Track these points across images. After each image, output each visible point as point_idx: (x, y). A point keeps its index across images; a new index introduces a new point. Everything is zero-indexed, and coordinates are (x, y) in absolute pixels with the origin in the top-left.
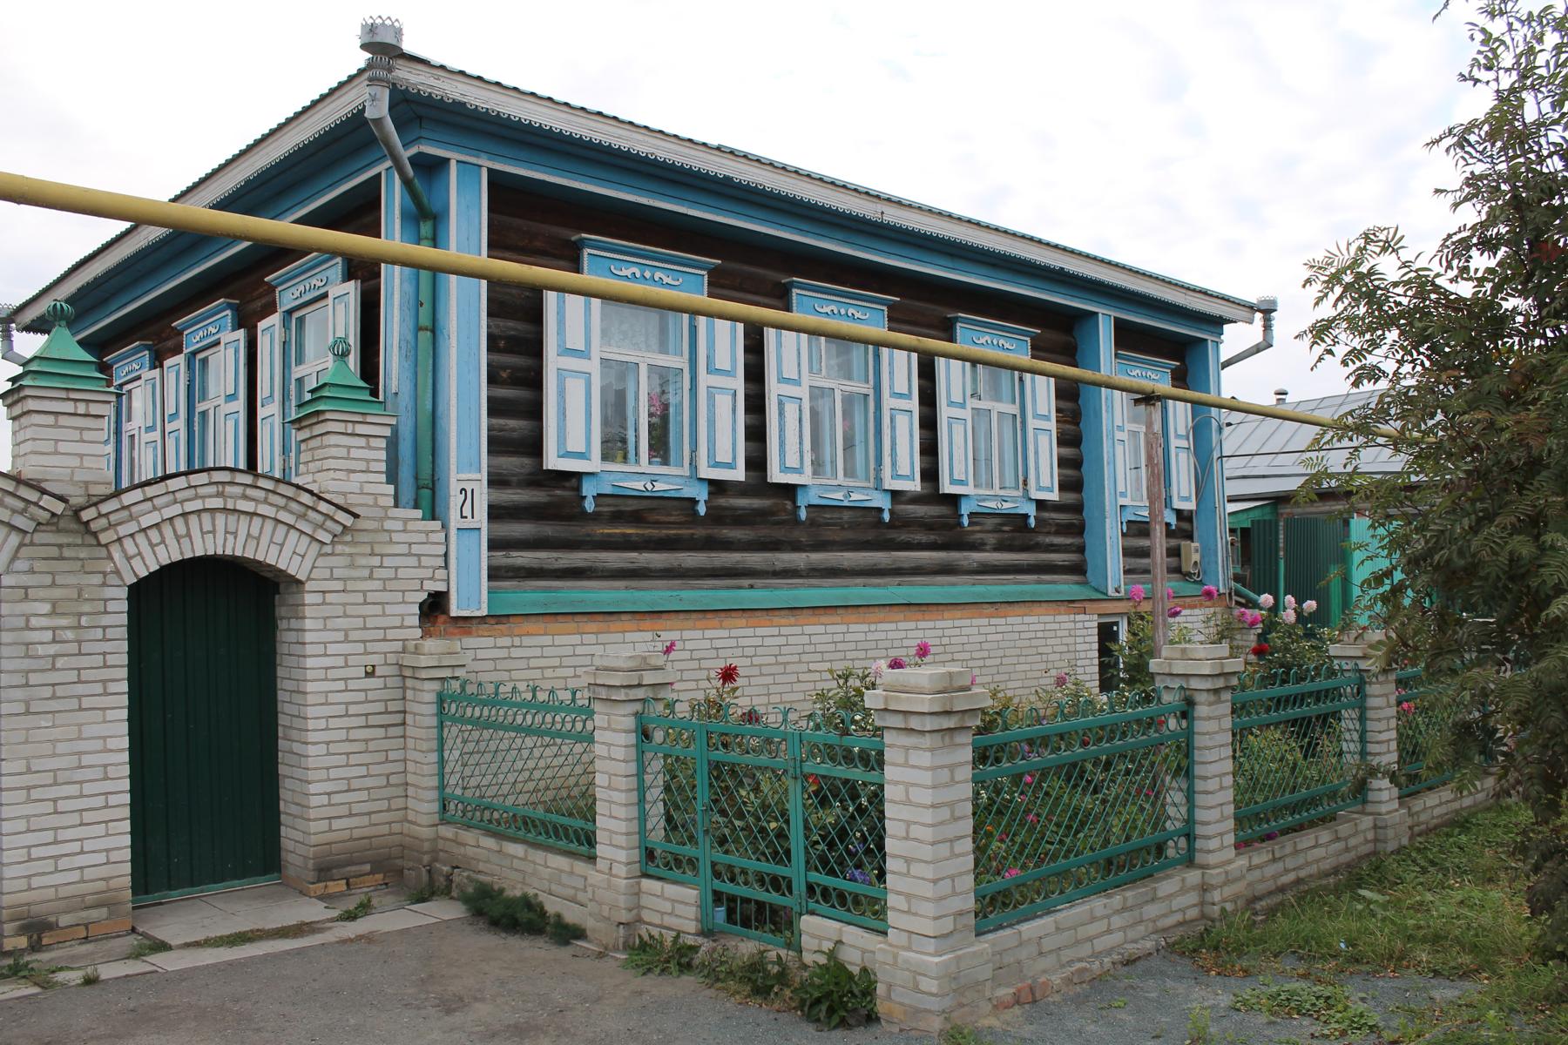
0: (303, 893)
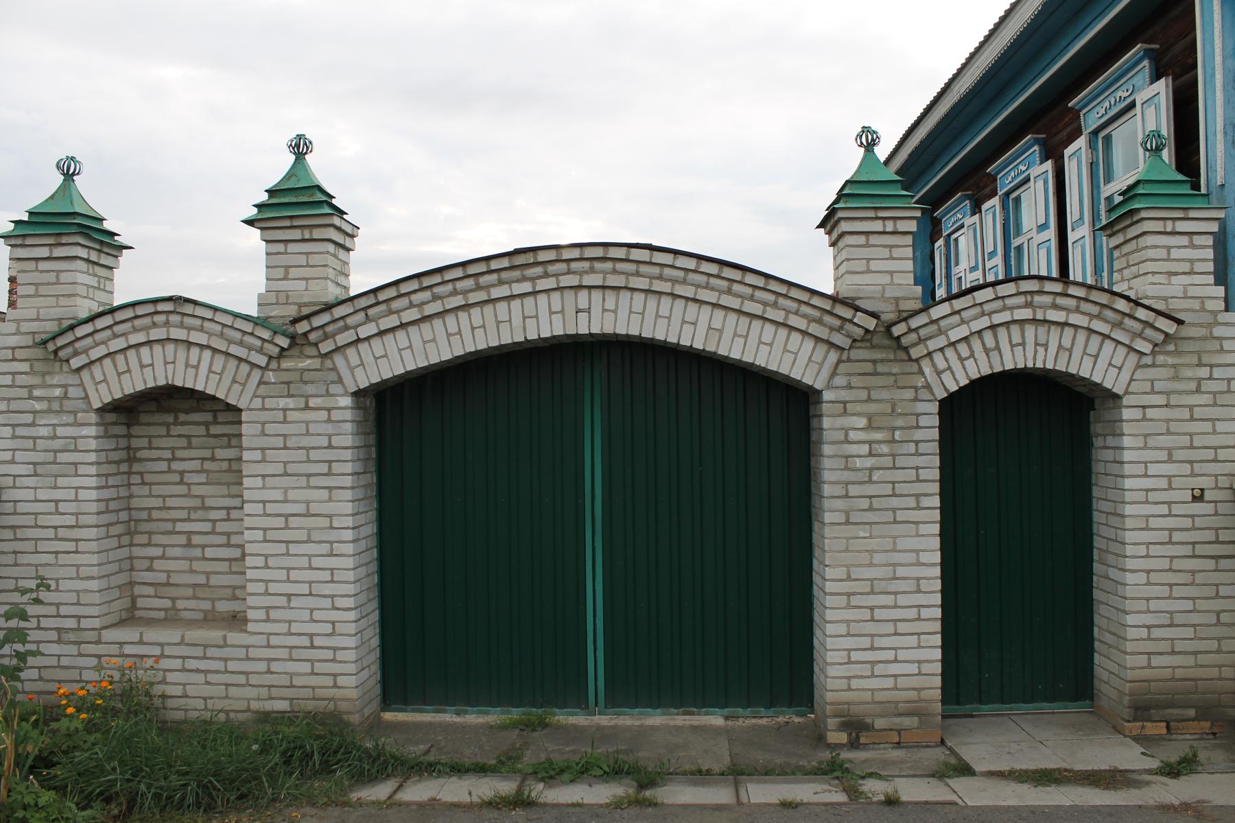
0: (1117, 730)
